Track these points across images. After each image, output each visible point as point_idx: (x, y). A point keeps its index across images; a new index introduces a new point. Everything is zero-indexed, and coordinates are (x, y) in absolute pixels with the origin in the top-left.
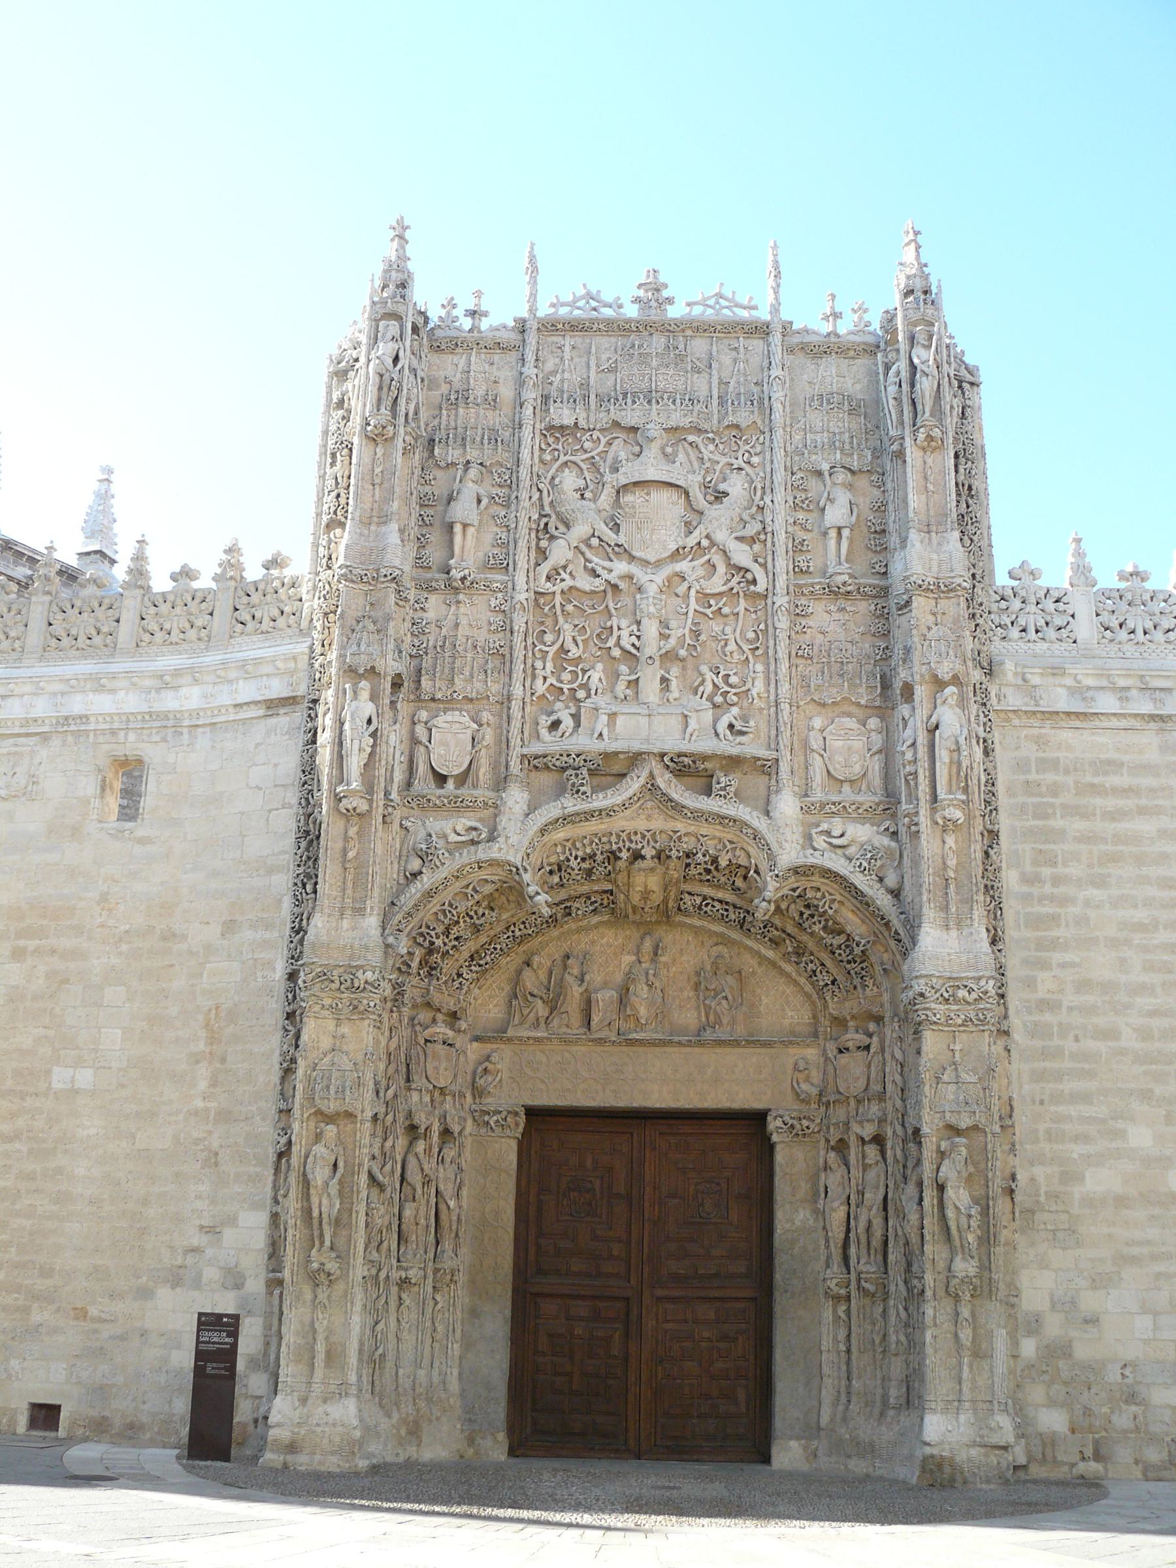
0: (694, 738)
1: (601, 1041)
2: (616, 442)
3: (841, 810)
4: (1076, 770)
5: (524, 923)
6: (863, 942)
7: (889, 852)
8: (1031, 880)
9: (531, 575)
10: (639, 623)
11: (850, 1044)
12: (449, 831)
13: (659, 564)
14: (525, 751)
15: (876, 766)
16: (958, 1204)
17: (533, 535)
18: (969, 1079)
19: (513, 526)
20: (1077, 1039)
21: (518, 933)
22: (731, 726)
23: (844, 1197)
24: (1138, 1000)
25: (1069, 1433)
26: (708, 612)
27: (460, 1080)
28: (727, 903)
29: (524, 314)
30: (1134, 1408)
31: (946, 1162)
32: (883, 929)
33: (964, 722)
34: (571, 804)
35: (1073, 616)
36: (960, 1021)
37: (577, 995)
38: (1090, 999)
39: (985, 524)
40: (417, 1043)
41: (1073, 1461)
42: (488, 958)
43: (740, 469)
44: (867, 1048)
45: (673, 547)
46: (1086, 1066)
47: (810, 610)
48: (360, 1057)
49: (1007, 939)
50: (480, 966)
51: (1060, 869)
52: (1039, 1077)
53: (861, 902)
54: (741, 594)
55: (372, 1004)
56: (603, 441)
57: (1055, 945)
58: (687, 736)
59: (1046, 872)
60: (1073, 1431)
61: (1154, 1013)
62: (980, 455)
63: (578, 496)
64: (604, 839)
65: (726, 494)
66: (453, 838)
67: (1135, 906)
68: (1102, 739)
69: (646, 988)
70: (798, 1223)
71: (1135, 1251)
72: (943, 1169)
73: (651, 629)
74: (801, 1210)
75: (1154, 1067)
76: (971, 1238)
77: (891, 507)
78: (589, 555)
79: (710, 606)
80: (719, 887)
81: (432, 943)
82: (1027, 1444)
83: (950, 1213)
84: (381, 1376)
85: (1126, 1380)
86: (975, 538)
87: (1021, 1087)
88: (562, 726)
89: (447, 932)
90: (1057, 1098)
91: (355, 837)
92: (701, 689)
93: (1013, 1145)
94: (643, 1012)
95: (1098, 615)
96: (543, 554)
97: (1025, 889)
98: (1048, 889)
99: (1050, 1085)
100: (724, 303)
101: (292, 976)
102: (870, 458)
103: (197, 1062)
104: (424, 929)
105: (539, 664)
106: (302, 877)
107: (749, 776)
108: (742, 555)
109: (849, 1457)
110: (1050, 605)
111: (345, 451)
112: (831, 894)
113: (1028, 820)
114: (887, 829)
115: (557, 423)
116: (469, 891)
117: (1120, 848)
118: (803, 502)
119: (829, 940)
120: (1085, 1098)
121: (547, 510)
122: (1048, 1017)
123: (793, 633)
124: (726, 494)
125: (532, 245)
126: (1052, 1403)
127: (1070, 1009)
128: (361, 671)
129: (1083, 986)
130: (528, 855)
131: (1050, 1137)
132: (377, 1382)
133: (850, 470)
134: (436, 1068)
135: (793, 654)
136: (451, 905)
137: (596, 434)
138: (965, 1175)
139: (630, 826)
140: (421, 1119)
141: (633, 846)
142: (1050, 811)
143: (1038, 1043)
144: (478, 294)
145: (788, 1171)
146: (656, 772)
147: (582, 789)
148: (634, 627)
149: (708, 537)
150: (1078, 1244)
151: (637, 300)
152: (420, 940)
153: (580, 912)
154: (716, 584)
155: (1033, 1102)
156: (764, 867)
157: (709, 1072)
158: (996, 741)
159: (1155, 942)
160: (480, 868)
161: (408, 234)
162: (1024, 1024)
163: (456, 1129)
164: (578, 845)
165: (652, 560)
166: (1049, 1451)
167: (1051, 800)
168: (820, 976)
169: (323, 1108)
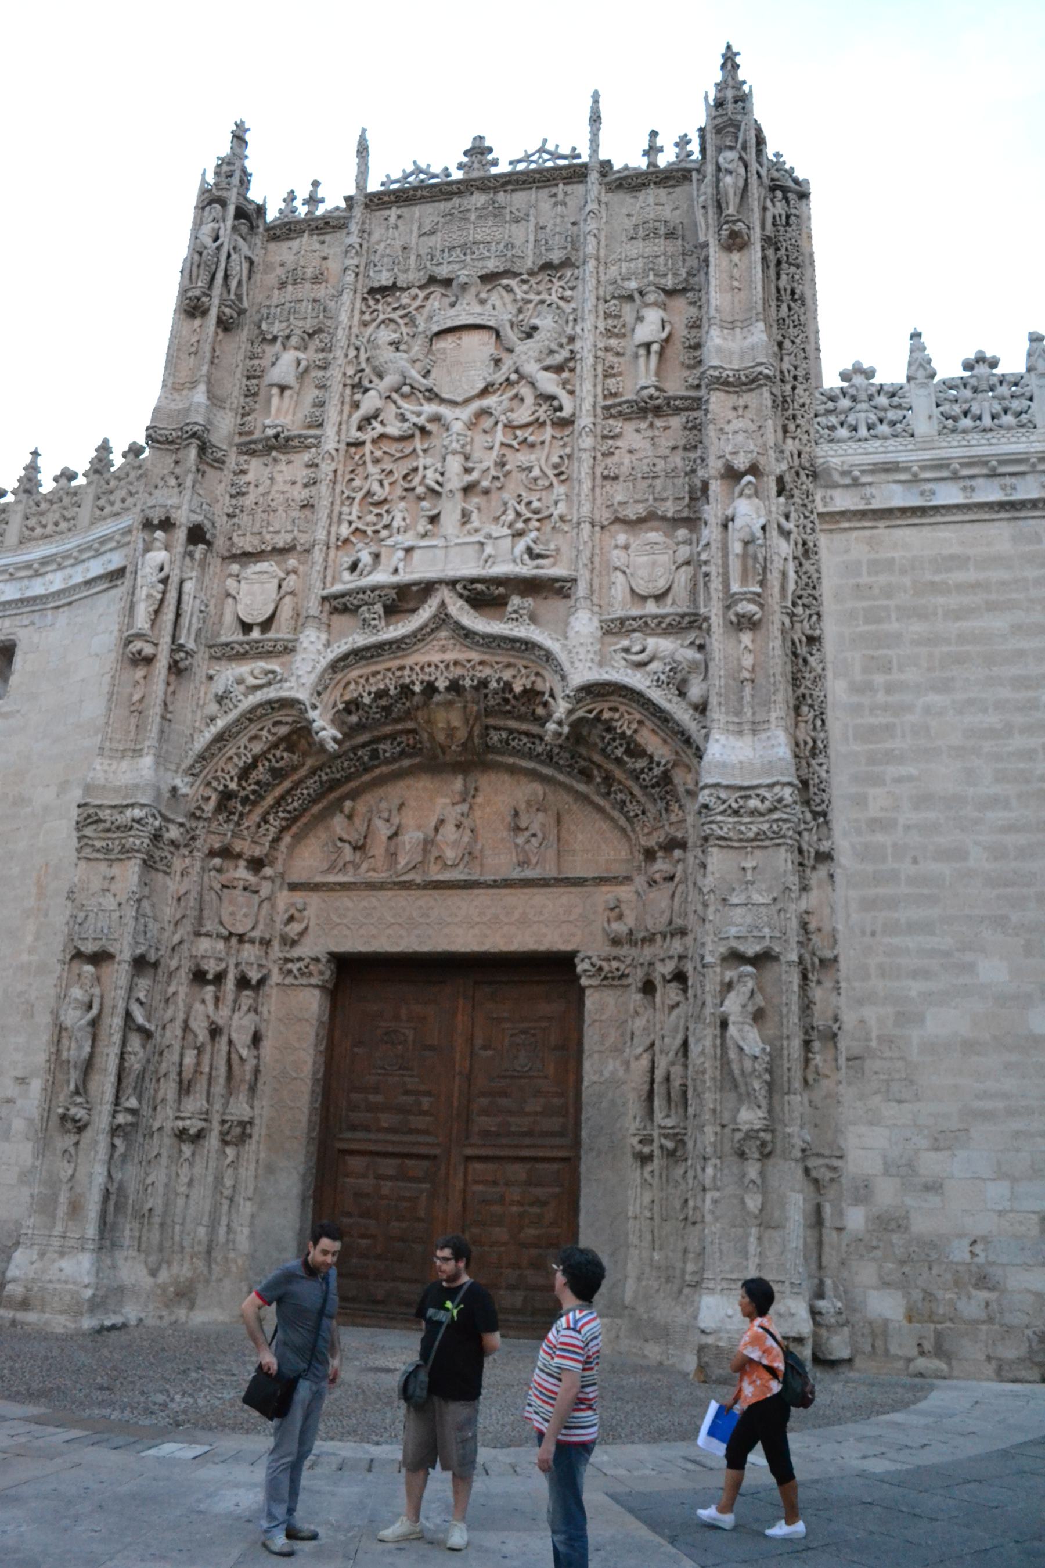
1: (406, 886)
3: (645, 626)
6: (663, 761)
7: (694, 666)
8: (864, 688)
9: (344, 427)
10: (444, 459)
11: (657, 876)
13: (467, 401)
14: (325, 593)
15: (683, 576)
16: (741, 1043)
17: (348, 391)
18: (762, 901)
20: (915, 861)
22: (529, 550)
23: (648, 1042)
24: (990, 815)
25: (905, 1323)
26: (515, 443)
27: (261, 926)
29: (352, 191)
30: (984, 1295)
31: (732, 995)
32: (684, 747)
33: (763, 512)
34: (361, 639)
36: (751, 835)
37: (384, 838)
38: (932, 815)
39: (812, 328)
40: (211, 888)
41: (910, 1355)
42: (296, 804)
44: (672, 878)
45: (481, 385)
46: (926, 891)
47: (618, 430)
48: (123, 898)
49: (831, 752)
50: (289, 812)
51: (895, 676)
52: (869, 905)
53: (659, 718)
54: (549, 422)
55: (138, 842)
56: (422, 295)
57: (890, 757)
58: (482, 562)
59: (879, 679)
60: (910, 1319)
61: (1010, 828)
62: (807, 262)
64: (398, 674)
65: (535, 328)
66: (251, 681)
67: (985, 711)
68: (945, 533)
69: (454, 829)
70: (606, 1074)
72: (727, 1003)
73: (454, 464)
74: (611, 1061)
75: (1009, 890)
76: (756, 1085)
78: (400, 402)
79: (516, 437)
80: (521, 718)
81: (226, 786)
82: (853, 1334)
83: (732, 1054)
84: (149, 1231)
85: (976, 1260)
86: (798, 341)
87: (848, 916)
88: (361, 566)
91: (142, 681)
93: (838, 982)
94: (450, 854)
95: (938, 405)
96: (356, 405)
97: (855, 699)
98: (881, 697)
100: (546, 156)
103: (28, 917)
104: (219, 773)
105: (346, 509)
107: (550, 602)
108: (548, 382)
109: (646, 1341)
110: (882, 400)
112: (629, 714)
113: (858, 626)
114: (692, 643)
115: (376, 285)
116: (265, 733)
119: (631, 763)
120: (926, 927)
121: (364, 365)
122: (880, 838)
124: (535, 328)
125: (364, 131)
126: (886, 1284)
127: (908, 828)
128: (156, 522)
129: (923, 800)
130: (319, 694)
131: (883, 973)
132: (144, 1239)
134: (232, 914)
136: (246, 747)
137: (414, 291)
138: (751, 1008)
139: (423, 659)
140: (211, 968)
141: (427, 678)
142: (883, 614)
143: (870, 868)
144: (316, 184)
145: (597, 1017)
146: (448, 600)
147: (373, 623)
149: (517, 371)
150: (917, 1097)
151: (460, 166)
152: (215, 784)
153: (388, 755)
154: (523, 415)
155: (863, 933)
157: (517, 915)
159: (1010, 749)
160: (273, 708)
161: (248, 137)
162: (853, 846)
163: (254, 976)
164: (372, 680)
166: (879, 1343)
167: (885, 602)
168: (630, 806)
169: (83, 949)
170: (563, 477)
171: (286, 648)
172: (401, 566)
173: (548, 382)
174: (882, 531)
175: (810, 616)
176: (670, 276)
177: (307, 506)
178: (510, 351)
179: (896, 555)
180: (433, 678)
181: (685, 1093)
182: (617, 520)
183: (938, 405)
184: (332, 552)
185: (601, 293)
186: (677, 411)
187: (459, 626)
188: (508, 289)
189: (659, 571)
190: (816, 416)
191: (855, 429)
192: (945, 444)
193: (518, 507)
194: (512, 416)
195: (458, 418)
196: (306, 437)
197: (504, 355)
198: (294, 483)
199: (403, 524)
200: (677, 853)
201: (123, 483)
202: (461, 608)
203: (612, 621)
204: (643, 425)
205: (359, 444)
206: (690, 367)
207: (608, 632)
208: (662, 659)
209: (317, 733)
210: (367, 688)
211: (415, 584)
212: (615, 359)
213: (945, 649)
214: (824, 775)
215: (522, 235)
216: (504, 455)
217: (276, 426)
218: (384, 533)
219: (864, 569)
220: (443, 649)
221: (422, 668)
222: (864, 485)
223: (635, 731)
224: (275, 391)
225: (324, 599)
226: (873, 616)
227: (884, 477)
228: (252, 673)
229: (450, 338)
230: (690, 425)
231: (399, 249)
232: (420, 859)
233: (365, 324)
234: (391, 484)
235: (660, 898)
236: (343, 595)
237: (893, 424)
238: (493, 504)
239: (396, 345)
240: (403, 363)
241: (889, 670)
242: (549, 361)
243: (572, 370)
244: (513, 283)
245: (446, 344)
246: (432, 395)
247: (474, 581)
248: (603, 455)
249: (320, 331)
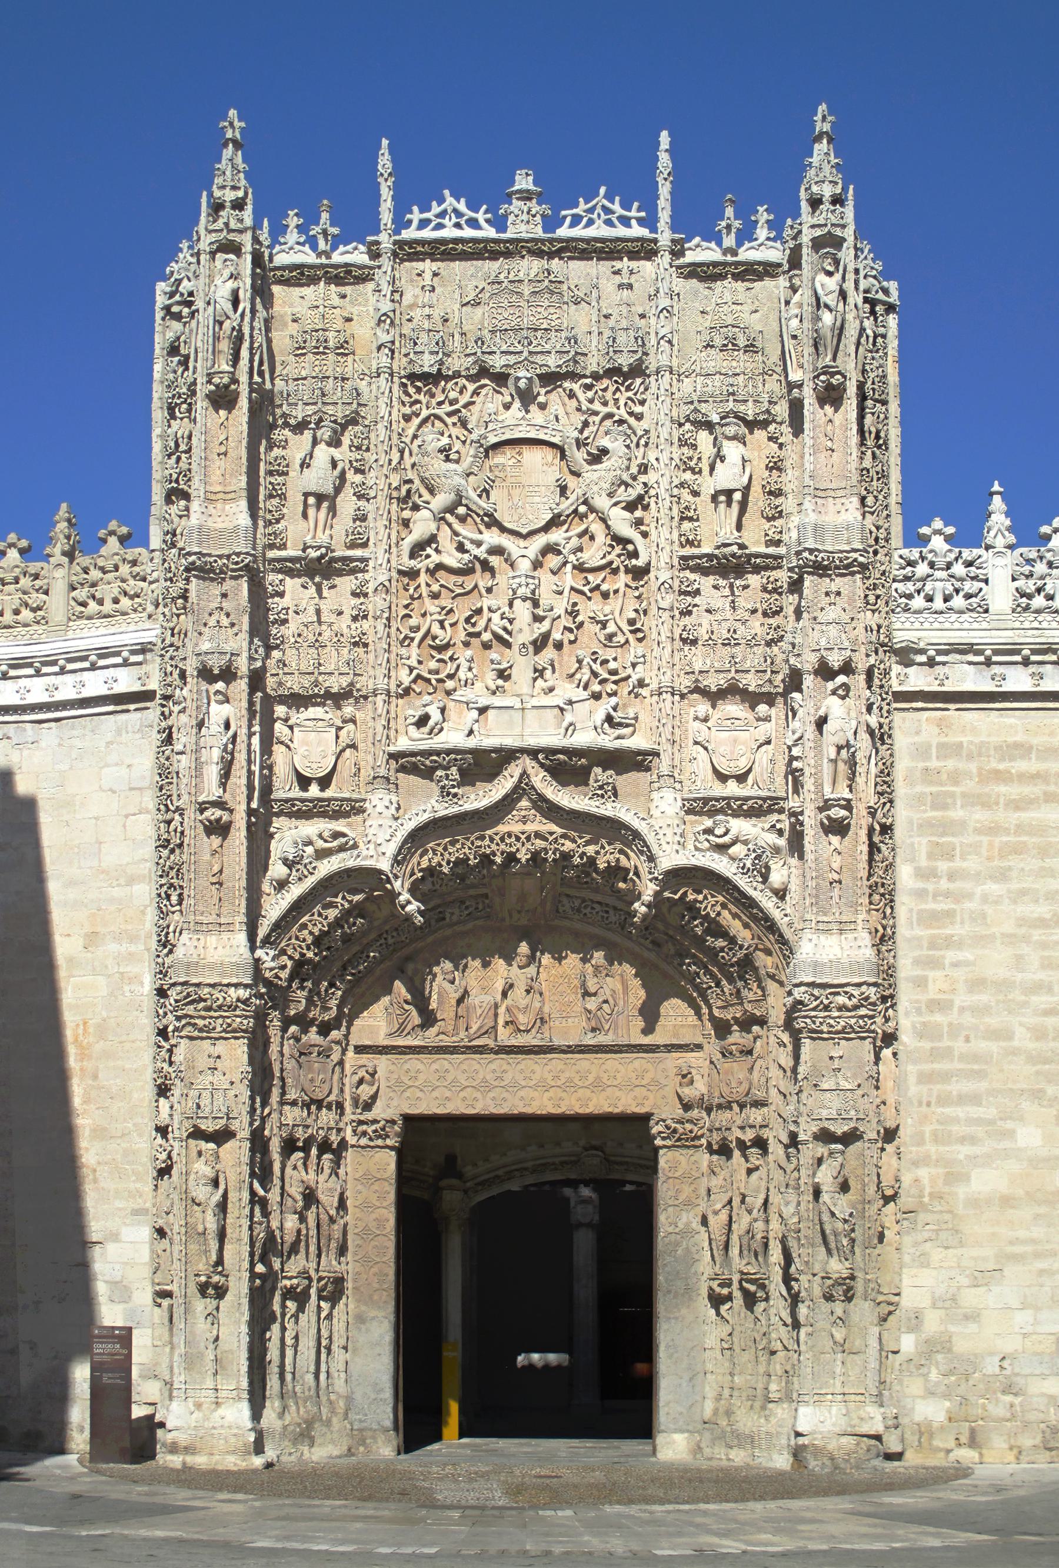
0: (570, 732)
2: (484, 392)
4: (980, 755)
5: (396, 929)
6: (746, 945)
9: (394, 550)
10: (511, 605)
12: (315, 838)
14: (392, 749)
17: (394, 507)
19: (372, 494)
20: (967, 1040)
21: (390, 941)
24: (1035, 999)
26: (586, 589)
28: (607, 905)
30: (1008, 1398)
35: (986, 581)
37: (454, 1002)
38: (984, 998)
43: (621, 422)
44: (750, 1052)
46: (976, 1067)
47: (696, 586)
49: (898, 937)
51: (958, 864)
52: (926, 1078)
54: (622, 568)
57: (949, 942)
58: (563, 731)
59: (943, 866)
63: (442, 457)
65: (604, 452)
66: (320, 844)
68: (1012, 719)
71: (1018, 1249)
73: (523, 611)
77: (787, 464)
78: (457, 526)
81: (303, 955)
86: (881, 497)
88: (431, 723)
89: (318, 941)
90: (944, 1100)
92: (578, 676)
95: (1014, 579)
96: (406, 523)
97: (920, 885)
98: (944, 884)
99: (939, 1086)
101: (161, 993)
102: (766, 404)
106: (165, 888)
108: (621, 522)
110: (959, 569)
111: (185, 406)
112: (713, 896)
113: (925, 811)
114: (773, 826)
115: (418, 370)
116: (339, 899)
117: (1024, 838)
118: (690, 459)
120: (975, 1099)
121: (410, 475)
122: (938, 1018)
123: (677, 613)
124: (604, 452)
126: (931, 1393)
127: (962, 1009)
129: (977, 984)
131: (936, 1139)
133: (743, 420)
135: (677, 636)
142: (949, 801)
143: (927, 1045)
146: (530, 771)
147: (453, 791)
148: (506, 609)
149: (585, 502)
150: (961, 1244)
154: (593, 556)
155: (920, 1104)
156: (644, 868)
158: (895, 724)
162: (914, 1027)
165: (524, 531)
170: (640, 635)
171: (353, 808)
172: (476, 727)
173: (621, 522)
174: (952, 713)
175: (884, 804)
176: (750, 404)
177: (359, 643)
178: (577, 474)
179: (964, 739)
180: (513, 849)
181: (766, 1245)
182: (697, 690)
183: (1014, 579)
184: (393, 700)
185: (675, 414)
186: (757, 570)
187: (542, 798)
188: (572, 395)
189: (741, 748)
190: (894, 581)
191: (930, 599)
192: (1017, 625)
193: (594, 666)
194: (584, 556)
195: (524, 552)
196: (351, 559)
197: (571, 482)
198: (340, 613)
199: (470, 675)
200: (756, 1028)
201: (110, 576)
202: (543, 779)
203: (695, 800)
204: (722, 582)
205: (413, 574)
206: (769, 519)
207: (690, 812)
208: (746, 843)
209: (403, 907)
210: (447, 856)
211: (496, 750)
212: (690, 498)
213: (1005, 839)
214: (892, 961)
215: (581, 319)
216: (575, 604)
217: (320, 547)
218: (450, 684)
219: (934, 751)
220: (524, 820)
221: (502, 839)
222: (939, 663)
223: (719, 914)
224: (311, 500)
225: (393, 756)
226: (940, 803)
227: (958, 657)
228: (320, 836)
229: (509, 452)
230: (770, 587)
231: (440, 322)
232: (492, 1024)
233: (407, 418)
234: (452, 625)
235: (737, 1069)
236: (413, 754)
237: (968, 596)
238: (566, 658)
239: (445, 451)
240: (459, 480)
241: (951, 858)
242: (623, 494)
243: (646, 508)
244: (576, 387)
245: (503, 458)
246: (492, 522)
247: (555, 751)
248: (682, 613)
249: (354, 422)
